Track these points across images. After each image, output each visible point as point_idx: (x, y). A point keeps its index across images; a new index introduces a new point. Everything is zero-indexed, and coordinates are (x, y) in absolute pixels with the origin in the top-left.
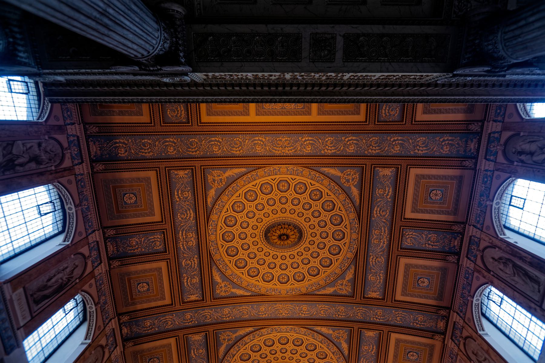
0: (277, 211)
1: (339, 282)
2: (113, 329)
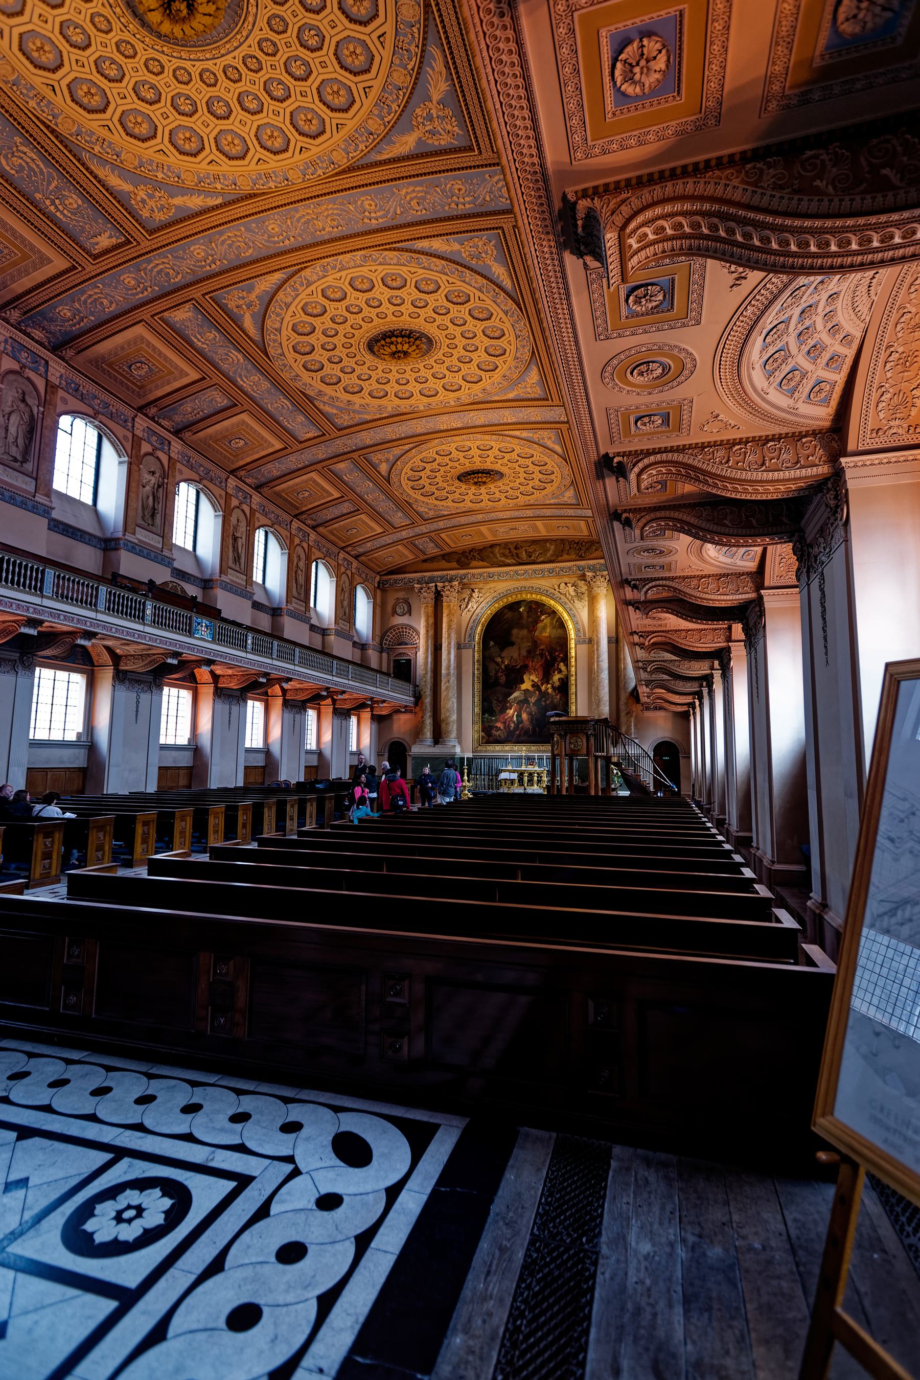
1: (418, 110)
2: (11, 337)
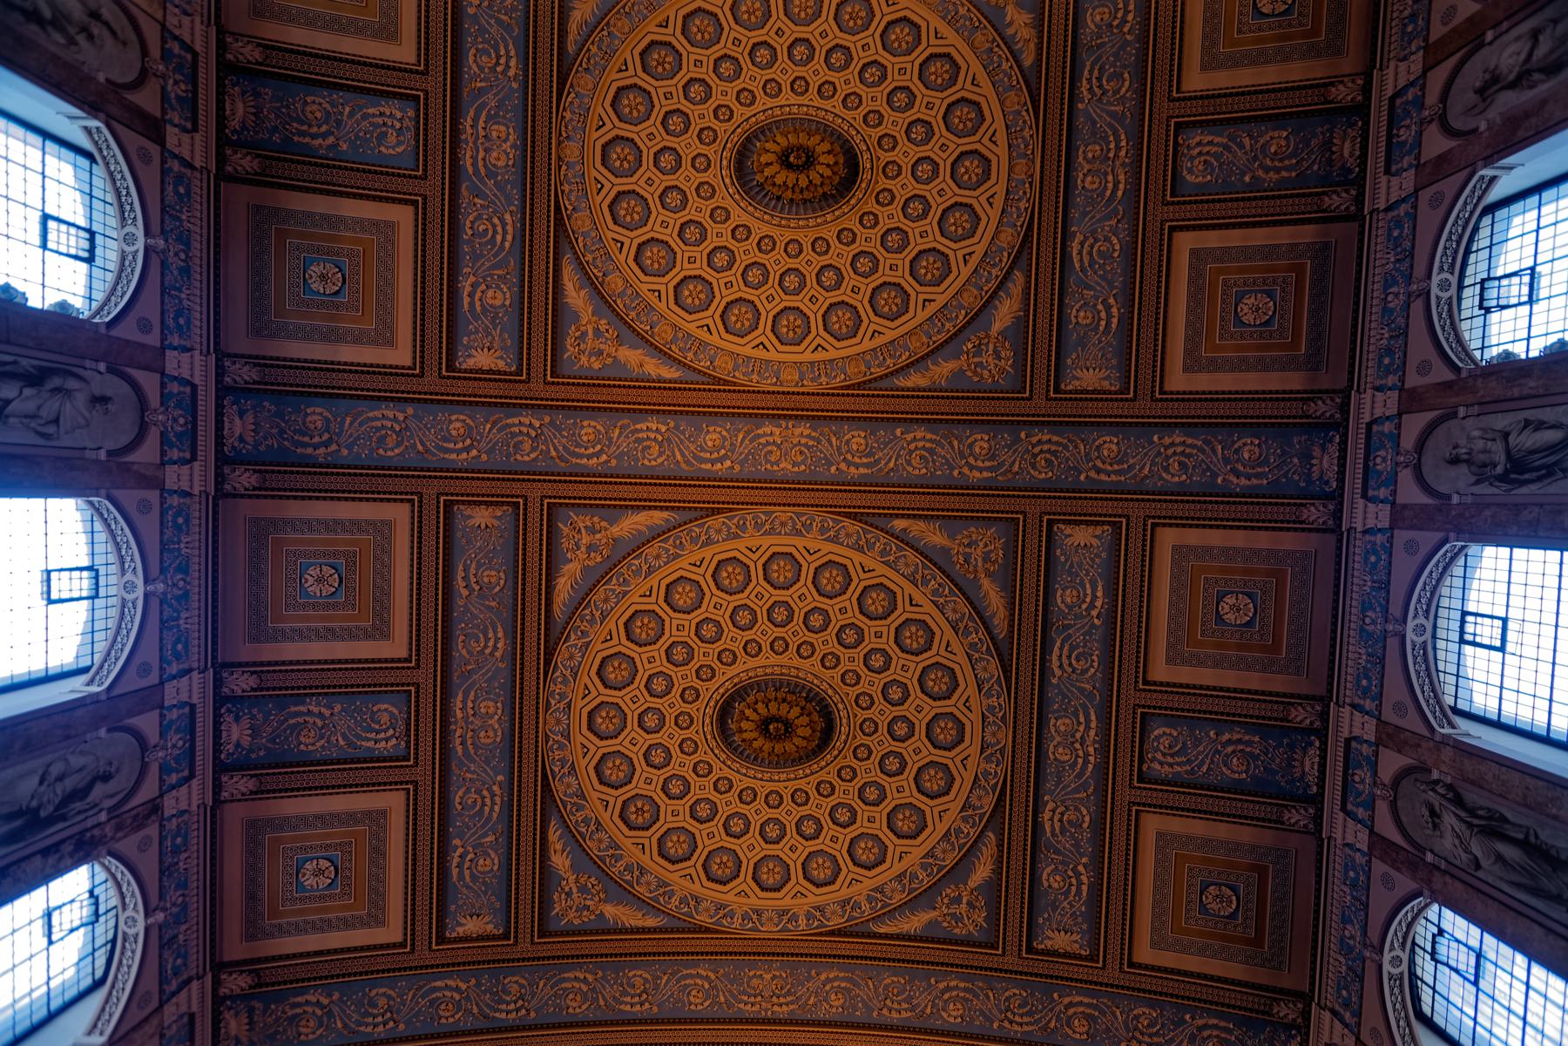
0: (760, 648)
